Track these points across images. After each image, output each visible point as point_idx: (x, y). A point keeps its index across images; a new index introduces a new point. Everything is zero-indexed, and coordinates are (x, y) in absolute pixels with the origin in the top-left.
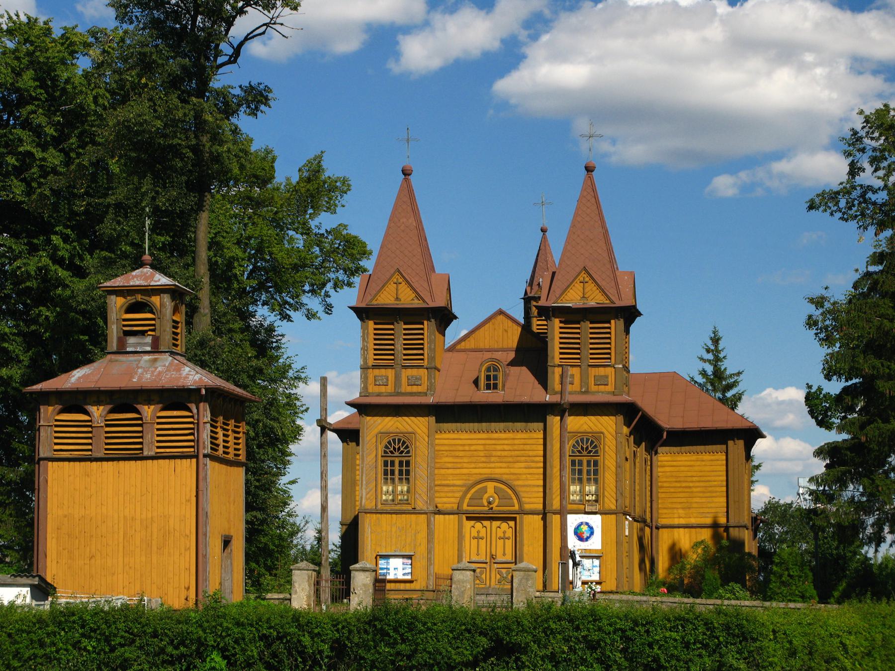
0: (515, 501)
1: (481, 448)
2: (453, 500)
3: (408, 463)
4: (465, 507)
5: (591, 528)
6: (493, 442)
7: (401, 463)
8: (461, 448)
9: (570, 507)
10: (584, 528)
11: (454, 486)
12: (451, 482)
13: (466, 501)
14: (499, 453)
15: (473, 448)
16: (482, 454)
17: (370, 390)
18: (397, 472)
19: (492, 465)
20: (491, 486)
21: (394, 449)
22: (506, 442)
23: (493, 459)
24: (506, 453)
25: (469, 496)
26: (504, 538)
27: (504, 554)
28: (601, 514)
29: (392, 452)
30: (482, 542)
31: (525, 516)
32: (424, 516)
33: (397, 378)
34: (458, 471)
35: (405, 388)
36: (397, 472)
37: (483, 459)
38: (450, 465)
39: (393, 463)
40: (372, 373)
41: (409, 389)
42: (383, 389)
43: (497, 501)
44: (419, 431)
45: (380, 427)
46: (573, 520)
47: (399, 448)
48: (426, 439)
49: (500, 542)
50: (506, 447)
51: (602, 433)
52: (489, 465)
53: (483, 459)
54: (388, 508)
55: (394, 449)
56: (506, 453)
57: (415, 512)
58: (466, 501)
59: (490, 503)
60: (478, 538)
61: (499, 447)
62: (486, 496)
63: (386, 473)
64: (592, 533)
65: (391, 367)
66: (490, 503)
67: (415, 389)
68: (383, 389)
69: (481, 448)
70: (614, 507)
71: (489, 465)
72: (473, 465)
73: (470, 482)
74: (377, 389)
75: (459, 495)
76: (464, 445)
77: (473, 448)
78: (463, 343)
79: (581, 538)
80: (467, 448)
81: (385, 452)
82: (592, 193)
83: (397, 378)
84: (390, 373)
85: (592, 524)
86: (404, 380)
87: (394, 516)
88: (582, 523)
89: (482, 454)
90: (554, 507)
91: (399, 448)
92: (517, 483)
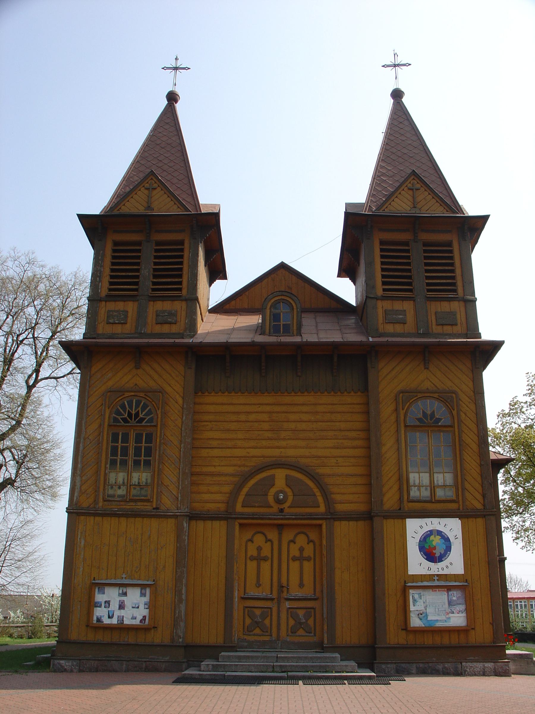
0: (320, 499)
1: (265, 417)
2: (218, 497)
3: (149, 438)
4: (239, 508)
5: (447, 540)
6: (284, 408)
7: (138, 439)
8: (234, 417)
9: (407, 506)
10: (436, 540)
11: (220, 474)
12: (218, 469)
13: (241, 498)
14: (292, 426)
15: (252, 417)
16: (266, 426)
17: (100, 331)
18: (131, 452)
19: (283, 443)
20: (280, 475)
21: (130, 415)
22: (305, 409)
23: (283, 434)
24: (304, 426)
25: (245, 490)
26: (301, 559)
27: (301, 585)
28: (460, 517)
29: (125, 420)
30: (266, 566)
31: (337, 523)
32: (172, 521)
33: (141, 315)
34: (228, 452)
35: (152, 327)
36: (131, 452)
37: (269, 434)
38: (215, 443)
39: (126, 439)
40: (104, 308)
41: (158, 329)
42: (118, 329)
43: (290, 498)
44: (168, 389)
45: (110, 383)
46: (415, 528)
47: (137, 414)
48: (180, 401)
49: (295, 566)
50: (305, 417)
51: (454, 392)
52: (276, 443)
53: (269, 434)
54: (115, 507)
55: (130, 415)
56: (304, 426)
57: (157, 514)
58: (241, 498)
59: (278, 501)
60: (259, 559)
61: (292, 417)
62: (273, 491)
63: (114, 451)
64: (448, 549)
65: (133, 298)
66: (278, 501)
67: (166, 329)
68: (118, 329)
69: (265, 417)
70: (479, 506)
71: (276, 443)
72: (252, 443)
73: (246, 469)
74: (109, 329)
75: (227, 489)
76: (238, 413)
77: (252, 417)
78: (233, 302)
79: (430, 555)
80: (243, 417)
81: (116, 420)
82: (404, 116)
83: (141, 315)
84: (131, 307)
85: (446, 531)
86: (151, 317)
87: (123, 520)
88: (431, 532)
89: (266, 426)
90: (386, 507)
91: (137, 414)
92: (321, 471)
